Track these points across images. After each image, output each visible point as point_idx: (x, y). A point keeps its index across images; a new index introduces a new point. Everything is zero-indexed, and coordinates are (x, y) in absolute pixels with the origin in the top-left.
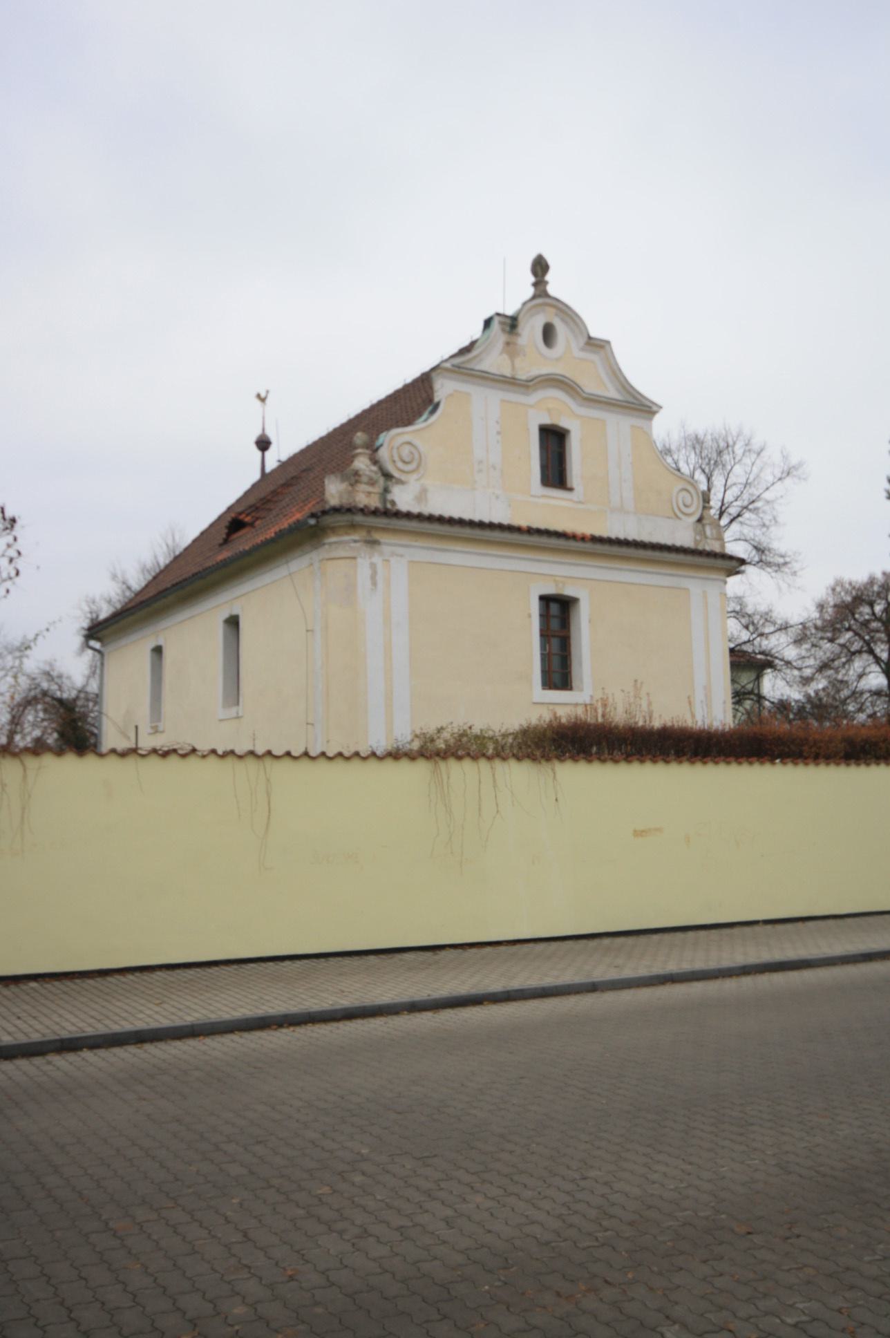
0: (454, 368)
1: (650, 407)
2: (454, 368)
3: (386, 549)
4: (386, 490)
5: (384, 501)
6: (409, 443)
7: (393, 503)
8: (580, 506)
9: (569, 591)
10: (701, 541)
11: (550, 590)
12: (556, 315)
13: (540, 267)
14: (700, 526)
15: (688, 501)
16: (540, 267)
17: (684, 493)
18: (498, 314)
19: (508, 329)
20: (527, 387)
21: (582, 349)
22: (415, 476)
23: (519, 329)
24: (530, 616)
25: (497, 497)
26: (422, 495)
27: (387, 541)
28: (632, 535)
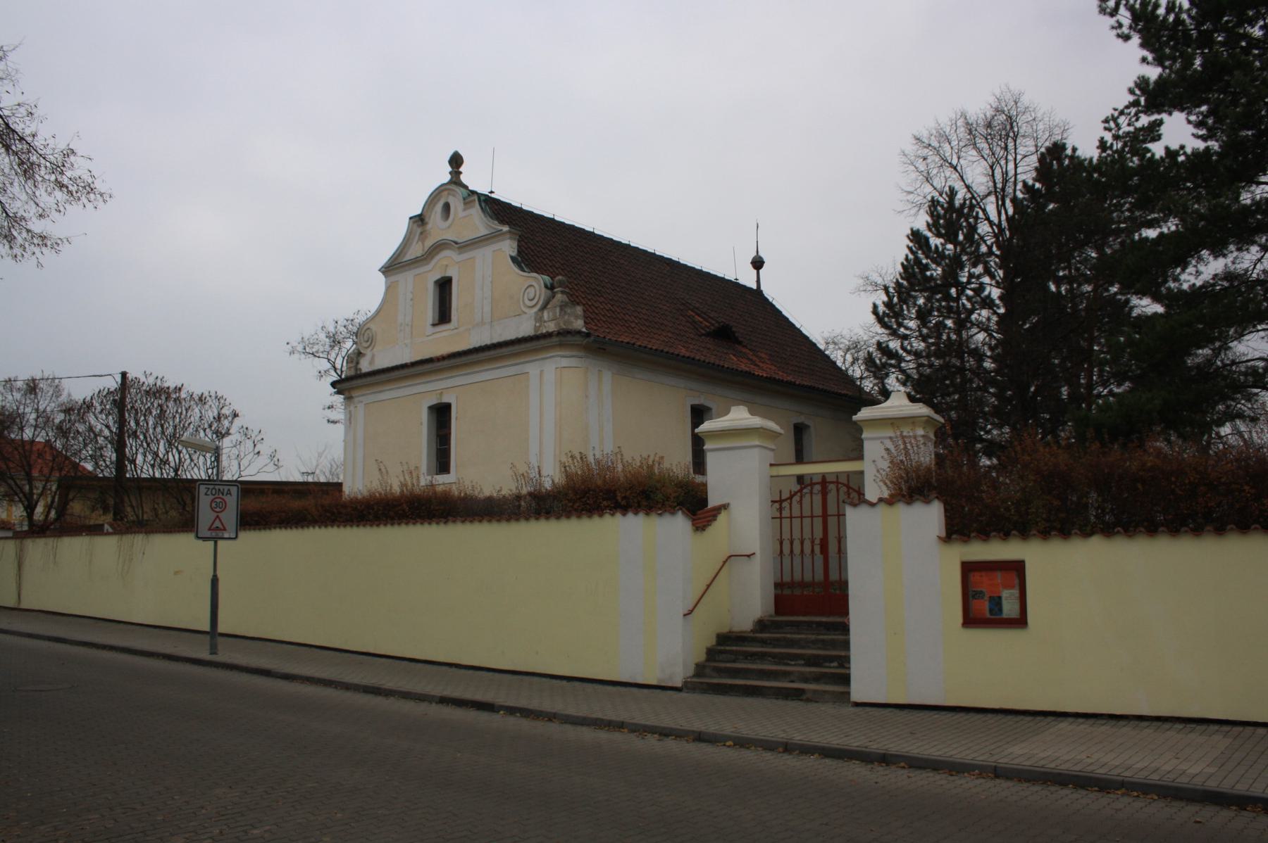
0: (387, 269)
1: (501, 230)
2: (387, 269)
3: (356, 400)
4: (358, 363)
5: (356, 369)
6: (368, 329)
7: (360, 369)
8: (456, 331)
9: (445, 400)
10: (540, 326)
11: (434, 401)
12: (449, 194)
13: (456, 161)
14: (540, 313)
15: (532, 296)
16: (456, 161)
17: (527, 291)
18: (411, 218)
19: (420, 223)
20: (425, 259)
21: (464, 210)
23: (427, 220)
24: (421, 424)
25: (407, 346)
26: (372, 362)
27: (356, 395)
28: (487, 341)
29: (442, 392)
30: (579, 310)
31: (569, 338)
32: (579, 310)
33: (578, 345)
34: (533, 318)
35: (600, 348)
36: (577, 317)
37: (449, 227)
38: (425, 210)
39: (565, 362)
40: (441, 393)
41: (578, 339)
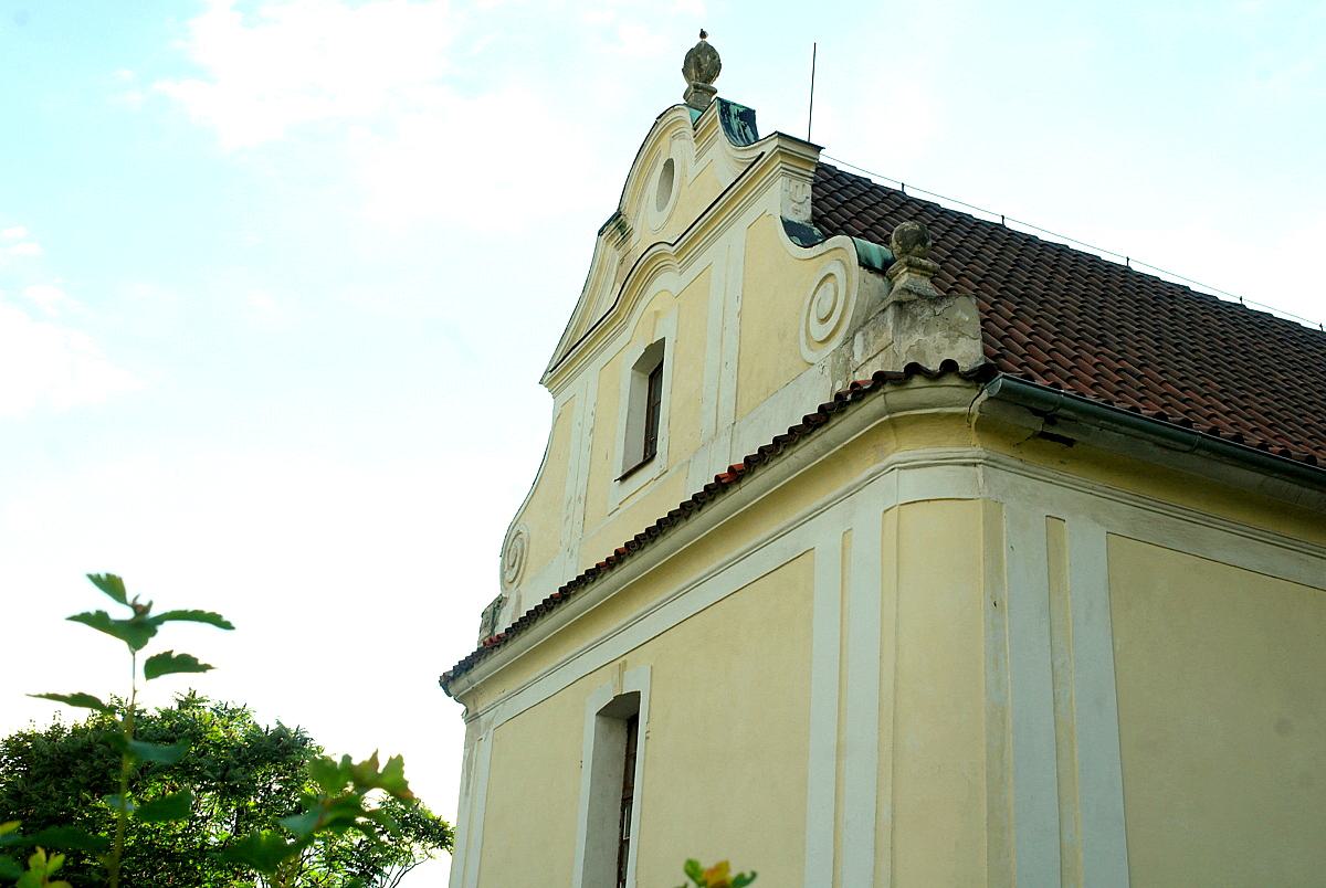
1: (763, 153)
3: (483, 718)
16: (702, 64)
22: (516, 583)
23: (630, 224)
29: (625, 662)
30: (966, 312)
31: (919, 390)
32: (966, 312)
33: (962, 416)
34: (827, 371)
35: (1043, 435)
36: (955, 331)
37: (669, 218)
38: (625, 200)
39: (911, 484)
40: (623, 667)
41: (950, 389)
